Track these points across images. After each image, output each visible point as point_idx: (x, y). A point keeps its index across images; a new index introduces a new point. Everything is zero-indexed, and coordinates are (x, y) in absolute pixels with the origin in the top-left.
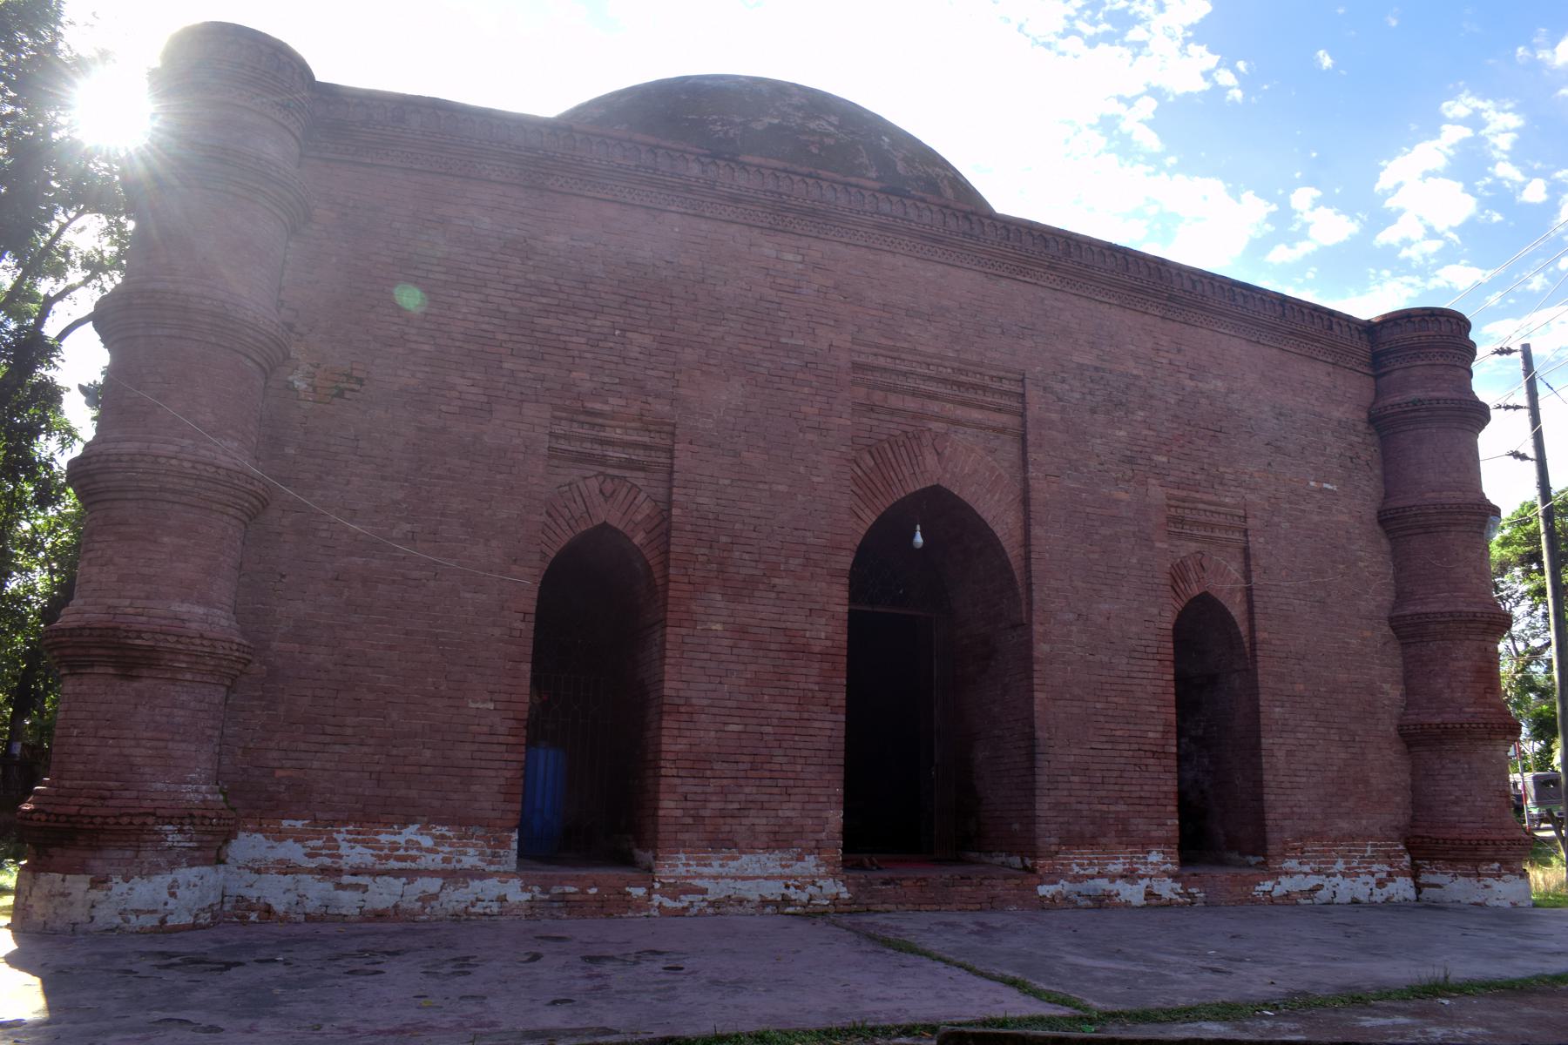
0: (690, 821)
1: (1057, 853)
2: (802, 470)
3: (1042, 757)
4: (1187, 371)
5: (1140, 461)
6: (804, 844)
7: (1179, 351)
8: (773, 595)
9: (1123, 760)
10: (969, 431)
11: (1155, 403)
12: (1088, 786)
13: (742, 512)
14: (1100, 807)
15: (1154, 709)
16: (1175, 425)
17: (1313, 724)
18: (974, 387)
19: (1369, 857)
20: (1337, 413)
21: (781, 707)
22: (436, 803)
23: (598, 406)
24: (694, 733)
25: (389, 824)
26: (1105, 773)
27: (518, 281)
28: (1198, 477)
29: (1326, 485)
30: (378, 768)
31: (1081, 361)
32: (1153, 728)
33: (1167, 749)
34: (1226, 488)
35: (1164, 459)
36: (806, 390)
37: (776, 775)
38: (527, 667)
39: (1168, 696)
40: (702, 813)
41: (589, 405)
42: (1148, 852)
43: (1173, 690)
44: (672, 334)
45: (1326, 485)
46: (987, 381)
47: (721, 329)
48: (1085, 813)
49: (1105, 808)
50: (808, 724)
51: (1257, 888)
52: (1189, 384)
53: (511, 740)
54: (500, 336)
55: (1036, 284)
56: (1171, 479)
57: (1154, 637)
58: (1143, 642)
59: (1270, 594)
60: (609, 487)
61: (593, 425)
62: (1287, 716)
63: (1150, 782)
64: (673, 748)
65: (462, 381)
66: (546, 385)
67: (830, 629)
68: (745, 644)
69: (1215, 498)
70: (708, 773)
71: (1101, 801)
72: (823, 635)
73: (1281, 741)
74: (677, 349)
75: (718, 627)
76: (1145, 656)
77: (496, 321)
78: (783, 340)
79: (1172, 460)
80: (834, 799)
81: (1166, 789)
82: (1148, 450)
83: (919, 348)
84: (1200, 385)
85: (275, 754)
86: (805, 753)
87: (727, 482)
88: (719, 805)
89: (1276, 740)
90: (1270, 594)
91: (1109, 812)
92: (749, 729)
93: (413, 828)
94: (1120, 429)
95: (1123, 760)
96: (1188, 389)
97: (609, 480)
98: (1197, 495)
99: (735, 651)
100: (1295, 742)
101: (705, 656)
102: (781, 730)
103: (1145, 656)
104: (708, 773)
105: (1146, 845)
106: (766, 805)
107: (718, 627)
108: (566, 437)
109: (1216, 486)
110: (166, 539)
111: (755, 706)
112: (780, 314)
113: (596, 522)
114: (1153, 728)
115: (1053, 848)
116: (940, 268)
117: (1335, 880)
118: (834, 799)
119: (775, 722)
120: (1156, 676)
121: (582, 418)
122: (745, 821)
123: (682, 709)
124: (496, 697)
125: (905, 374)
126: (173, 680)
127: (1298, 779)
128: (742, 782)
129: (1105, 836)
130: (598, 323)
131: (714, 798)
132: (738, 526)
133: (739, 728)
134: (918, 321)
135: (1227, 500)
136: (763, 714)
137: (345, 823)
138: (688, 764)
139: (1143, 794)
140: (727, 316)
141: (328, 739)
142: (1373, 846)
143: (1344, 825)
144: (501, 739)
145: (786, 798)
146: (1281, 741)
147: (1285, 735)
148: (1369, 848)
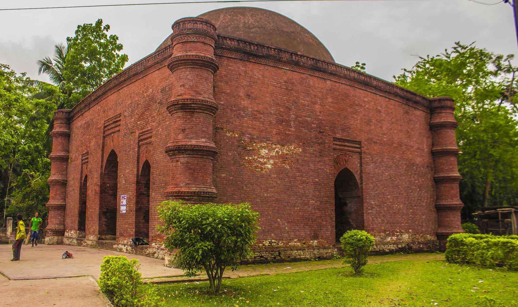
46: (118, 119)
69: (147, 129)
125: (110, 125)
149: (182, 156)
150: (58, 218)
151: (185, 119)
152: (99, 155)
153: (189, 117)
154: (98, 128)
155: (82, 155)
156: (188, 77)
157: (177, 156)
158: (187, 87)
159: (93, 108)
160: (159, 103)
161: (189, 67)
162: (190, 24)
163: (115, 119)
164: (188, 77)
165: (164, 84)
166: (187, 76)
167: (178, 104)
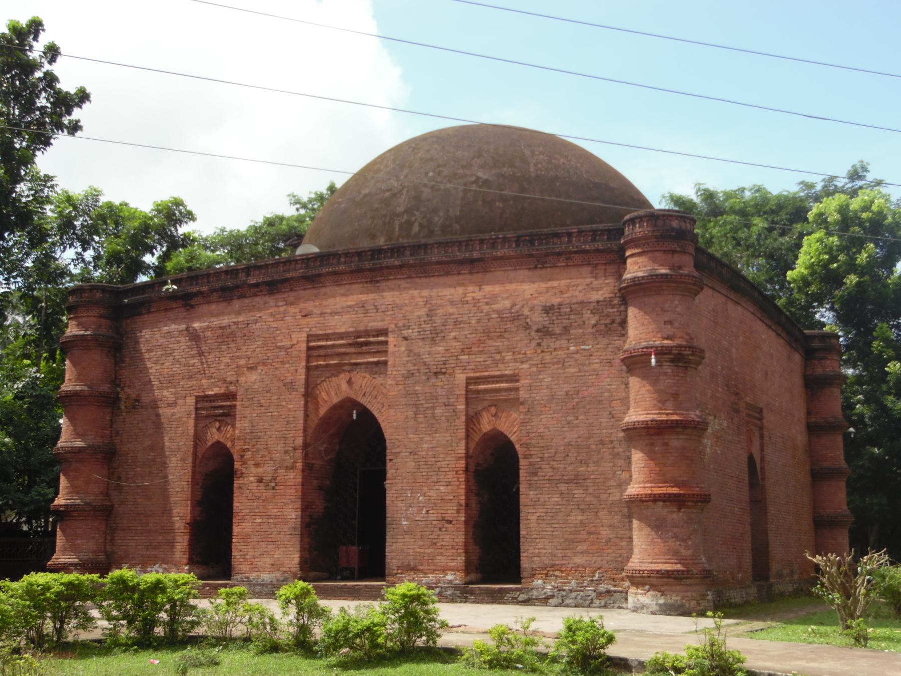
0: (242, 560)
1: (397, 574)
2: (284, 403)
3: (390, 526)
4: (485, 300)
5: (450, 362)
6: (284, 569)
7: (480, 290)
8: (272, 462)
9: (432, 526)
10: (363, 366)
11: (462, 325)
12: (413, 540)
13: (261, 427)
14: (419, 550)
15: (452, 498)
16: (474, 335)
17: (557, 499)
18: (367, 344)
19: (597, 580)
20: (595, 296)
21: (276, 510)
22: (163, 556)
23: (211, 393)
24: (243, 524)
25: (150, 564)
26: (423, 533)
27: (183, 347)
28: (487, 363)
29: (582, 347)
30: (146, 544)
31: (419, 313)
32: (451, 508)
33: (459, 519)
34: (507, 365)
35: (467, 357)
36: (287, 365)
37: (273, 540)
38: (189, 502)
39: (460, 491)
40: (247, 557)
41: (207, 393)
42: (446, 574)
43: (464, 487)
44: (237, 354)
45: (582, 347)
46: (372, 339)
47: (254, 346)
48: (411, 554)
49: (422, 551)
50: (285, 517)
51: (508, 595)
52: (486, 308)
53: (186, 531)
54: (179, 372)
55: (395, 279)
56: (470, 367)
57: (453, 459)
58: (447, 463)
59: (532, 424)
60: (217, 424)
61: (210, 401)
62: (539, 496)
63: (448, 537)
64: (237, 531)
65: (167, 394)
66: (194, 388)
67: (294, 474)
68: (261, 484)
69: (498, 373)
70: (249, 540)
71: (420, 547)
72: (292, 477)
73: (534, 511)
74: (238, 360)
75: (252, 479)
76: (447, 469)
77: (177, 366)
78: (279, 344)
79: (471, 356)
80: (296, 549)
81: (456, 540)
82: (456, 354)
83: (337, 331)
84: (493, 306)
85: (120, 541)
86: (285, 530)
87: (255, 415)
88: (253, 554)
89: (530, 511)
90: (532, 424)
91: (424, 553)
92: (264, 521)
93: (157, 565)
94: (440, 346)
95: (432, 526)
96: (485, 311)
97: (218, 423)
98: (486, 374)
99: (259, 488)
100: (545, 511)
101: (248, 491)
102: (275, 521)
103: (447, 469)
104: (249, 540)
105: (444, 571)
106: (270, 553)
107: (252, 479)
108: (203, 409)
109: (500, 365)
110: (71, 474)
111: (265, 511)
112: (278, 332)
113: (214, 440)
114: (451, 508)
115: (395, 572)
116: (347, 287)
117: (564, 593)
118: (296, 549)
119: (273, 517)
120: (454, 479)
121: (206, 399)
122: (262, 560)
123: (240, 514)
124: (181, 515)
125: (333, 346)
126: (76, 520)
127: (545, 533)
128: (261, 543)
129: (422, 565)
130: (210, 357)
131: (251, 550)
132: (259, 434)
133: (260, 520)
134: (336, 317)
135: (507, 372)
136: (269, 514)
137: (139, 564)
138: (241, 537)
139: (444, 543)
140: (257, 339)
141: (133, 535)
142: (599, 573)
143: (578, 560)
144: (182, 531)
145: (276, 549)
146: (534, 511)
147: (536, 507)
148: (597, 575)
149: (675, 437)
150: (94, 538)
151: (676, 378)
152: (295, 404)
153: (682, 375)
154: (279, 348)
155: (197, 397)
156: (678, 309)
157: (666, 437)
158: (676, 325)
159: (247, 301)
160: (538, 331)
161: (679, 293)
162: (676, 221)
163: (359, 337)
164: (678, 309)
165: (555, 301)
166: (676, 307)
167: (670, 353)
